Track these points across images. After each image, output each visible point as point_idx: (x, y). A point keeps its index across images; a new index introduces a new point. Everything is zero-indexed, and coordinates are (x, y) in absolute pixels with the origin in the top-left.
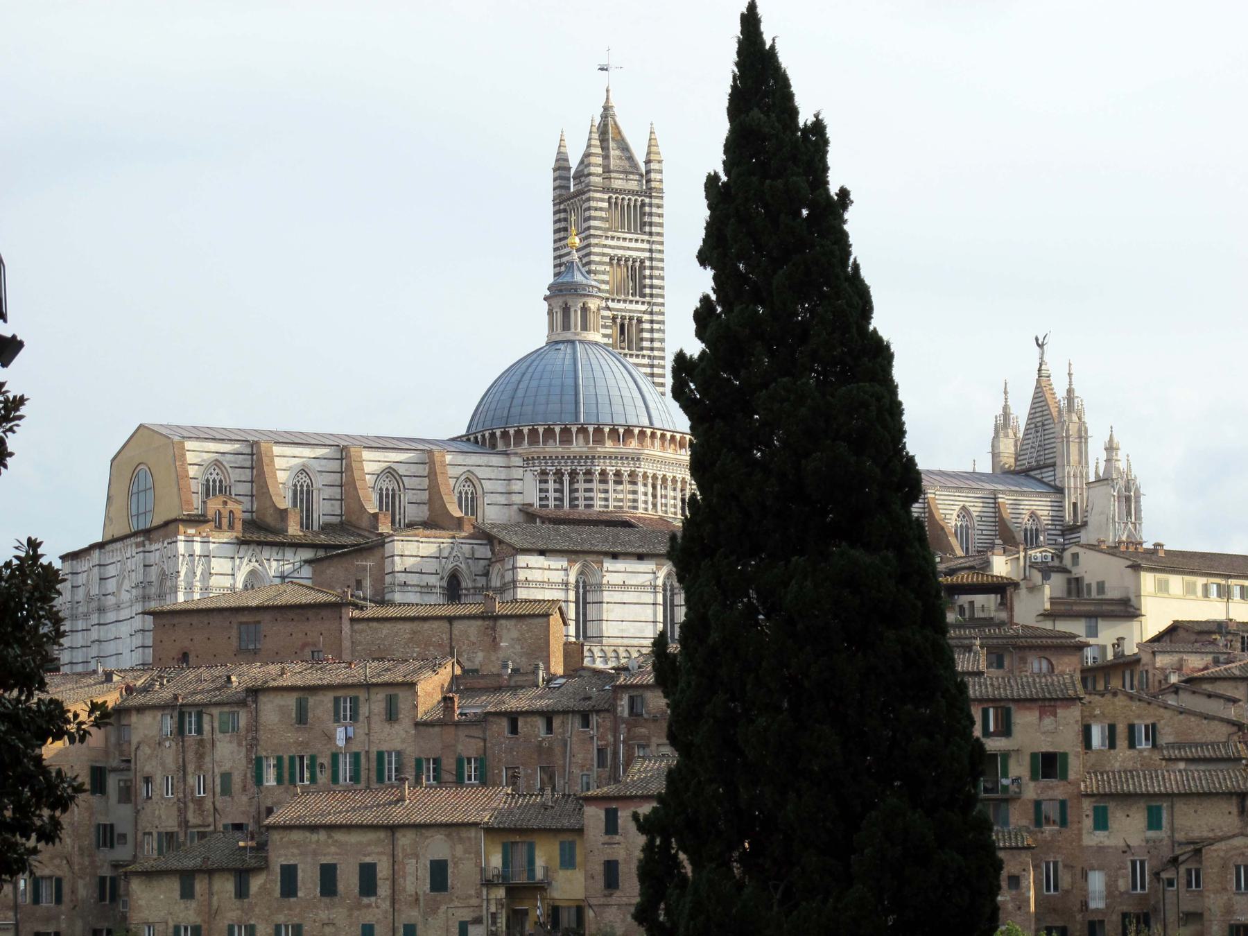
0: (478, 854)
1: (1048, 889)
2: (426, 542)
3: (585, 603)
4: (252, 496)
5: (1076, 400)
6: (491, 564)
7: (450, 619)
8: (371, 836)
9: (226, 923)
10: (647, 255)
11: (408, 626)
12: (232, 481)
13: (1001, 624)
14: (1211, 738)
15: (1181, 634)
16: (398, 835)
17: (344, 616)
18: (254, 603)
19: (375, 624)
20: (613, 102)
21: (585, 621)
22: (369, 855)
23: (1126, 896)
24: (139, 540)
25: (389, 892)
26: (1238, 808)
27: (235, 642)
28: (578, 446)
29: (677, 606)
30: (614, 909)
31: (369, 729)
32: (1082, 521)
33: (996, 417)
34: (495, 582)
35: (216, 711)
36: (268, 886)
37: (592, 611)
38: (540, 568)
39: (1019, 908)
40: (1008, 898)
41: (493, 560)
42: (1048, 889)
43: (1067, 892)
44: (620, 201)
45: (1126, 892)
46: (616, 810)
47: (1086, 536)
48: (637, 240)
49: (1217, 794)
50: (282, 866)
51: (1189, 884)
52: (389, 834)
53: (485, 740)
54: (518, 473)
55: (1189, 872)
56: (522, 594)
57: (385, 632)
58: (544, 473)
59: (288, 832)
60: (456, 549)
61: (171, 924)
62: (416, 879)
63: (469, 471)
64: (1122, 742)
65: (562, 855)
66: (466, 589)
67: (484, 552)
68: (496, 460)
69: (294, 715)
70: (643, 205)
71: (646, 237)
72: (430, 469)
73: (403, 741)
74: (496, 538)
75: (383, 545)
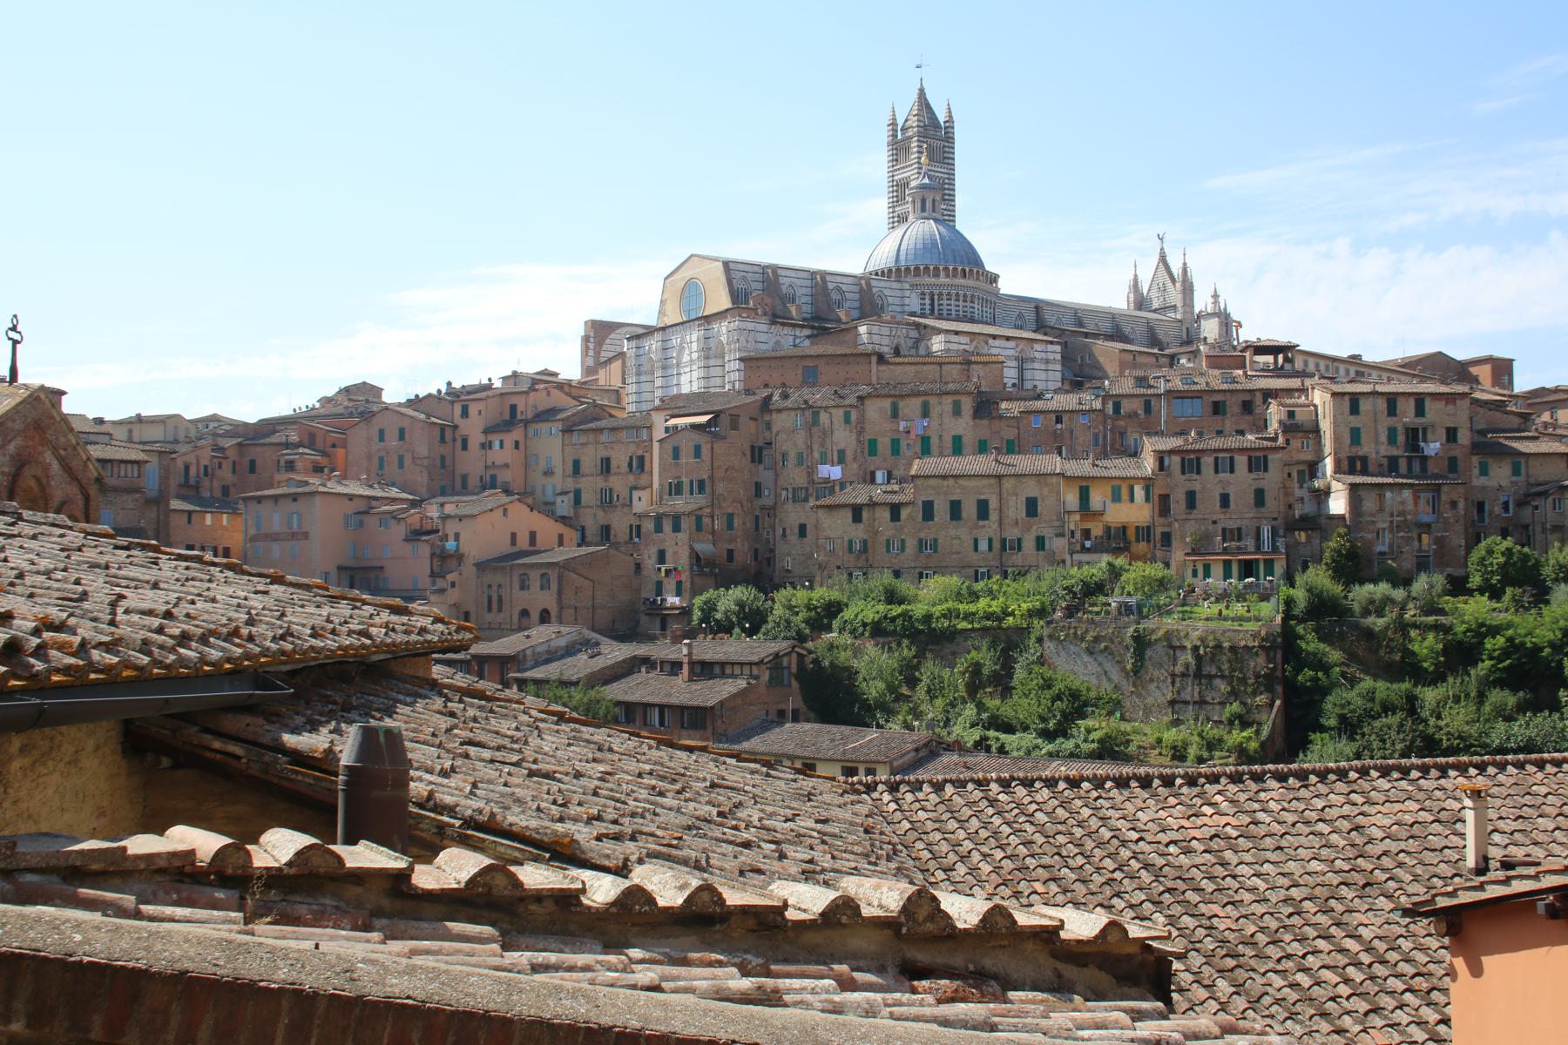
0: (1058, 493)
8: (985, 482)
11: (913, 368)
14: (1509, 426)
16: (1004, 481)
27: (800, 378)
28: (943, 280)
35: (832, 410)
54: (907, 293)
58: (923, 294)
61: (846, 539)
62: (1016, 509)
65: (1113, 494)
67: (914, 334)
68: (895, 285)
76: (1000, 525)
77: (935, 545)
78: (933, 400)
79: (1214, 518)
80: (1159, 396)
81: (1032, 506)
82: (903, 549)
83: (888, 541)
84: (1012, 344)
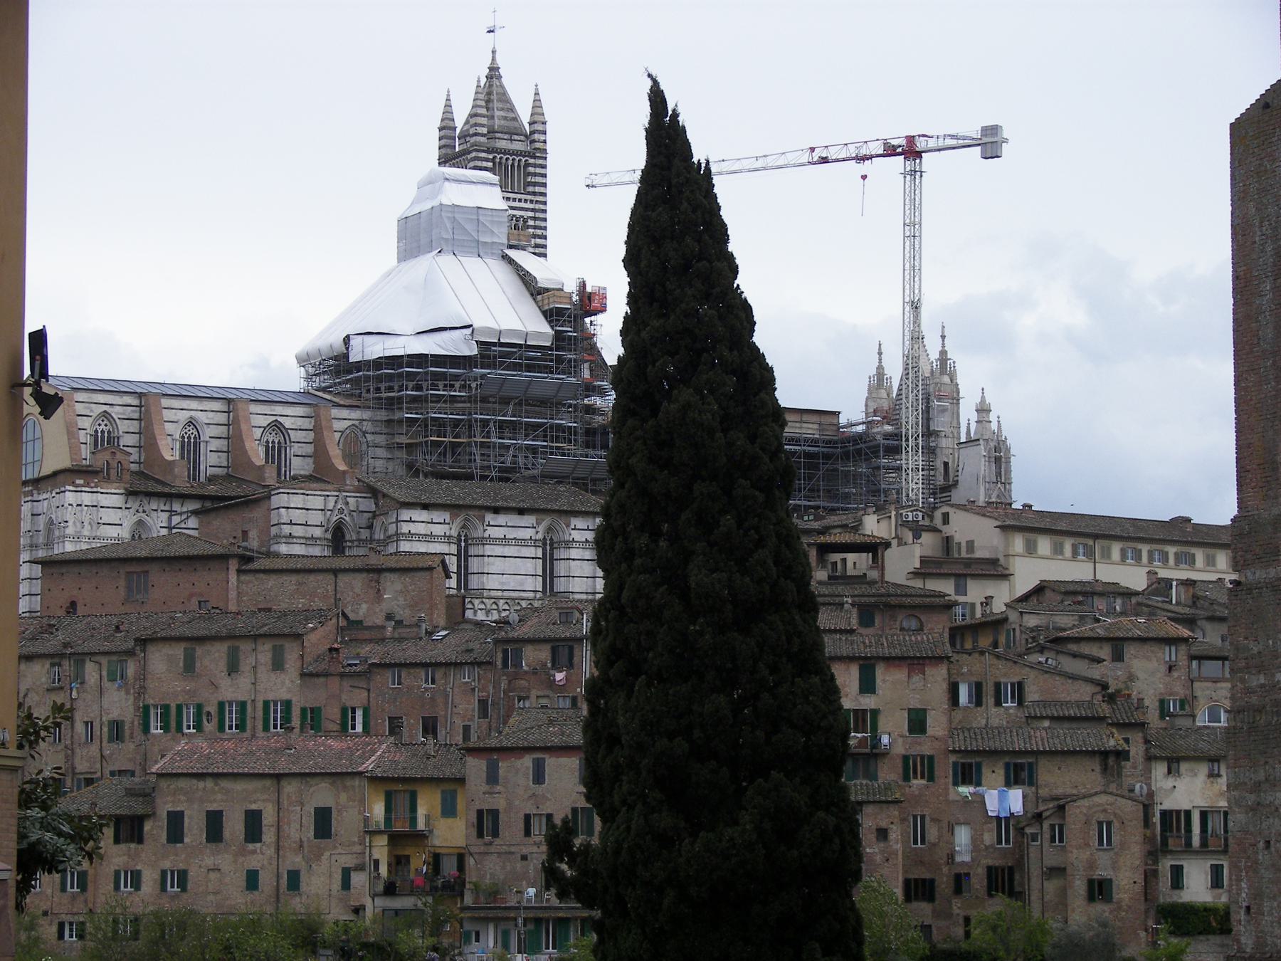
0: (362, 801)
1: (915, 842)
2: (311, 495)
3: (467, 556)
4: (140, 447)
5: (948, 362)
6: (375, 515)
7: (336, 572)
8: (258, 784)
9: (113, 868)
10: (531, 214)
11: (294, 578)
12: (121, 433)
13: (873, 583)
14: (1075, 697)
15: (1048, 594)
17: (231, 567)
18: (144, 554)
19: (262, 576)
20: (500, 62)
21: (467, 574)
22: (255, 802)
23: (991, 850)
24: (27, 489)
25: (274, 839)
26: (1101, 765)
27: (122, 591)
29: (557, 560)
30: (494, 857)
31: (255, 679)
32: (953, 481)
33: (870, 378)
34: (379, 535)
36: (155, 832)
37: (474, 564)
38: (423, 522)
39: (888, 860)
40: (877, 850)
41: (377, 513)
42: (915, 842)
43: (934, 845)
44: (504, 161)
45: (992, 846)
46: (497, 761)
47: (958, 496)
48: (520, 200)
49: (1081, 752)
50: (168, 812)
51: (1053, 840)
52: (275, 782)
53: (369, 690)
55: (1052, 827)
56: (405, 546)
57: (270, 584)
59: (175, 779)
60: (340, 501)
62: (300, 826)
63: (353, 425)
64: (989, 700)
66: (350, 541)
67: (368, 505)
69: (181, 664)
70: (527, 165)
71: (529, 197)
72: (316, 422)
73: (289, 691)
74: (380, 492)
75: (269, 497)
76: (278, 849)
77: (182, 878)
78: (245, 647)
79: (525, 851)
80: (581, 640)
81: (323, 822)
82: (137, 884)
83: (117, 873)
84: (530, 520)
